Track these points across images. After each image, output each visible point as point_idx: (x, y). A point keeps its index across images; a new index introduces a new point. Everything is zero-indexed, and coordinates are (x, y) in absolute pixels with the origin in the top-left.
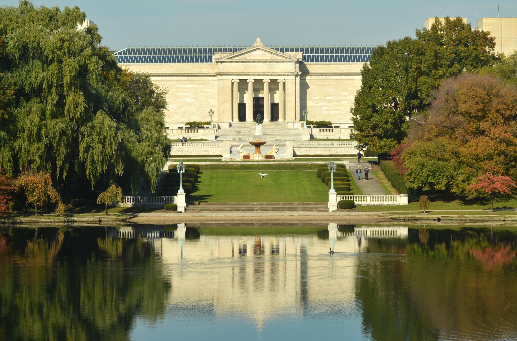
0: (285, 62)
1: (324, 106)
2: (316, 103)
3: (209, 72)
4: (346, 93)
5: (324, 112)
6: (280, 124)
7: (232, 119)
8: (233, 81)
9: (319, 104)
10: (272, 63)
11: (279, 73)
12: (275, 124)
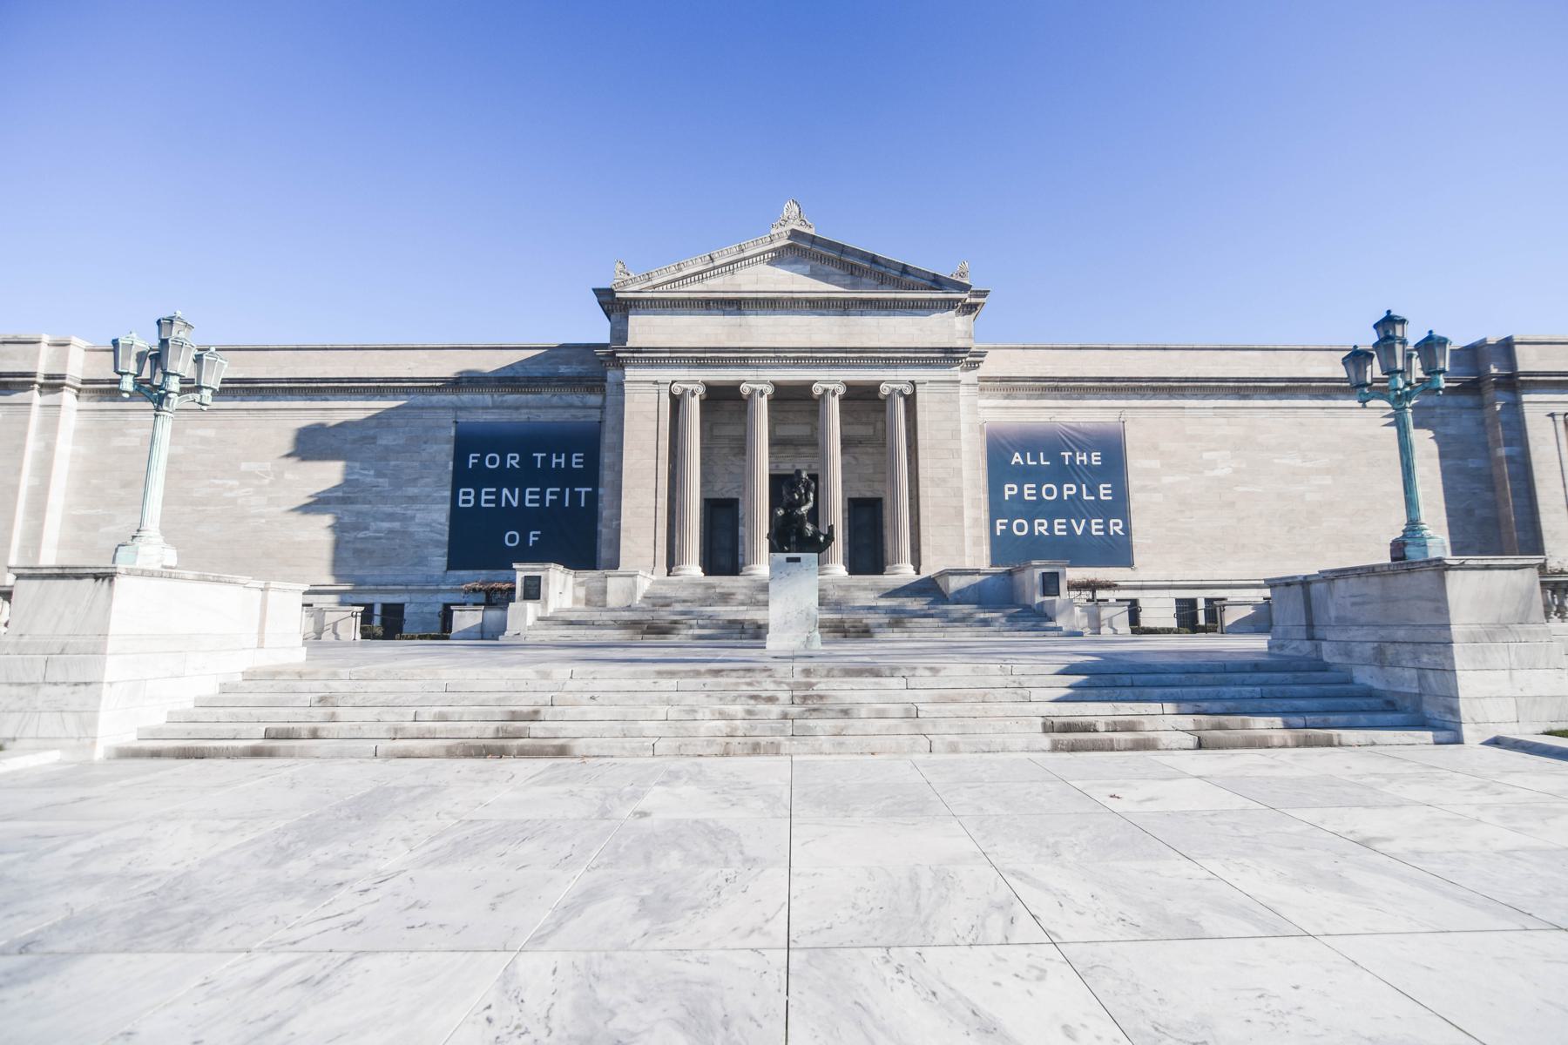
4: (1155, 464)
8: (677, 390)
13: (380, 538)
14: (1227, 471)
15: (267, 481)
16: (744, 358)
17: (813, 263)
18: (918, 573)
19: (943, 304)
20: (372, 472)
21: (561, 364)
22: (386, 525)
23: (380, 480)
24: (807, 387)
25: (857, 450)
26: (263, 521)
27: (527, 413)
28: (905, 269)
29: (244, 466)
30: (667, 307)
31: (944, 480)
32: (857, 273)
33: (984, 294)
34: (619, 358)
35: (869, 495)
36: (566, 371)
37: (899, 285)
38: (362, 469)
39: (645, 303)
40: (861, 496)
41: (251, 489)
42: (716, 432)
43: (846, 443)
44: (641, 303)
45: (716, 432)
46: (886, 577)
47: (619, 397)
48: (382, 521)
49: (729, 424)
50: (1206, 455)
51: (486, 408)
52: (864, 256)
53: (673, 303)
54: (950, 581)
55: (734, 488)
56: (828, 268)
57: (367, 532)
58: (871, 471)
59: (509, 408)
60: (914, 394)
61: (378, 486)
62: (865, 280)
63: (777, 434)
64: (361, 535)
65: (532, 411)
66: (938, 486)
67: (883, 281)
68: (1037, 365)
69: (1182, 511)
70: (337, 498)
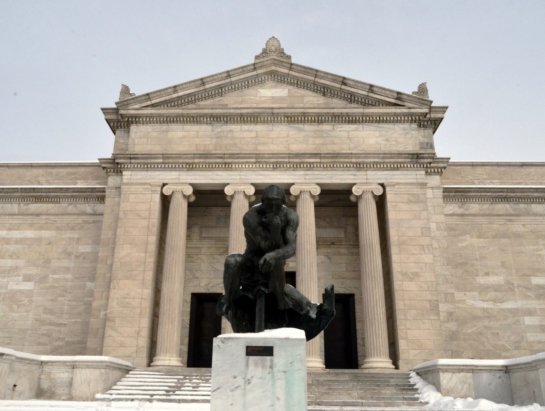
1: (530, 313)
2: (495, 301)
5: (531, 337)
8: (167, 191)
10: (326, 127)
11: (357, 156)
12: (357, 379)
16: (229, 163)
17: (290, 87)
18: (397, 368)
21: (80, 179)
24: (286, 189)
27: (46, 219)
31: (416, 274)
34: (118, 163)
43: (320, 243)
44: (141, 119)
46: (365, 371)
47: (117, 199)
49: (216, 227)
53: (168, 119)
54: (441, 378)
58: (344, 269)
59: (32, 215)
66: (411, 280)
68: (485, 179)
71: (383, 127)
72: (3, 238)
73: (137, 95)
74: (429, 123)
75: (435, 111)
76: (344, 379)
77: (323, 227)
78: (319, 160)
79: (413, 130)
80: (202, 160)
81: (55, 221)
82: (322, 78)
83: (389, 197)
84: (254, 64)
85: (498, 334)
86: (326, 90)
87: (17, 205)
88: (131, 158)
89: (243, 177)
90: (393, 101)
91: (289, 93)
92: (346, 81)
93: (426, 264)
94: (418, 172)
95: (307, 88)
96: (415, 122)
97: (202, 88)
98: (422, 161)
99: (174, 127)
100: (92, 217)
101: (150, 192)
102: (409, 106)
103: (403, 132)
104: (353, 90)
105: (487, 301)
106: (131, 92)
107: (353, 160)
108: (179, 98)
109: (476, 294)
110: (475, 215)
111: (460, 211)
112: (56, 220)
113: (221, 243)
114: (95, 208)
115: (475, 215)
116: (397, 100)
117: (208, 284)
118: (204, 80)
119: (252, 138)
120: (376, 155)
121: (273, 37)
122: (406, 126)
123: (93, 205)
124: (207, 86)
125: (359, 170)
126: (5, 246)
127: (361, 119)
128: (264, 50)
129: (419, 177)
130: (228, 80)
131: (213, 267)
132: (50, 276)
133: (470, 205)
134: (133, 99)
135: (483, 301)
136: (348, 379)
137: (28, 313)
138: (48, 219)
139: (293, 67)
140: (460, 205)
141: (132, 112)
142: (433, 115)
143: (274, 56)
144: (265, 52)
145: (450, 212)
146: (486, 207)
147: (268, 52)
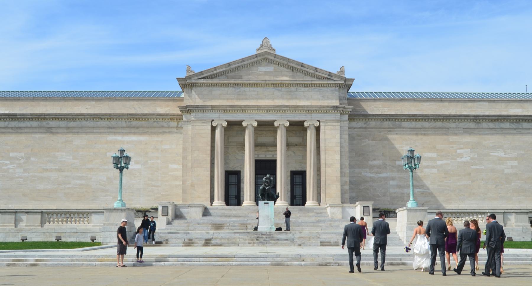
0: (321, 86)
3: (171, 112)
4: (434, 155)
6: (309, 210)
7: (212, 200)
8: (214, 124)
9: (382, 175)
10: (293, 89)
11: (307, 106)
12: (301, 210)
13: (76, 188)
14: (468, 159)
15: (22, 161)
16: (244, 110)
17: (275, 66)
19: (333, 85)
20: (71, 157)
22: (78, 182)
23: (75, 161)
25: (294, 149)
26: (22, 180)
28: (316, 69)
29: (12, 154)
30: (210, 86)
32: (295, 71)
33: (353, 80)
35: (300, 169)
36: (160, 110)
37: (313, 76)
38: (66, 156)
39: (200, 85)
40: (296, 170)
41: (15, 165)
42: (230, 140)
44: (198, 85)
45: (230, 140)
48: (77, 180)
50: (458, 151)
51: (123, 127)
52: (298, 63)
55: (239, 166)
56: (282, 68)
57: (70, 185)
59: (134, 127)
60: (319, 127)
61: (74, 164)
62: (298, 74)
63: (258, 141)
64: (67, 186)
65: (145, 129)
67: (306, 73)
69: (446, 177)
70: (56, 169)
71: (321, 89)
72: (120, 141)
73: (196, 72)
74: (345, 86)
75: (348, 81)
76: (296, 210)
77: (291, 136)
78: (288, 109)
79: (336, 91)
80: (231, 108)
81: (147, 131)
82: (291, 63)
83: (322, 127)
84: (256, 55)
85: (376, 189)
86: (293, 69)
87: (125, 122)
88: (195, 107)
89: (252, 116)
90: (327, 76)
91: (274, 69)
92: (303, 65)
93: (336, 160)
94: (336, 115)
95: (284, 67)
96: (338, 87)
97: (229, 68)
98: (338, 109)
99: (215, 88)
100: (168, 129)
101: (206, 125)
102: (335, 80)
103: (332, 92)
104: (307, 70)
105: (373, 173)
106: (192, 70)
107: (305, 109)
108: (216, 74)
109: (368, 169)
110: (372, 128)
111: (364, 126)
112: (148, 130)
113: (239, 145)
114: (169, 124)
115: (372, 128)
116: (329, 76)
117: (233, 166)
118: (230, 64)
119: (255, 95)
120: (316, 107)
121: (266, 37)
122: (333, 88)
123: (167, 122)
124: (232, 67)
125: (308, 113)
126: (122, 145)
127: (310, 85)
128: (261, 45)
129: (337, 117)
130: (243, 63)
131: (235, 157)
132: (149, 161)
133: (370, 122)
134: (193, 74)
135: (371, 173)
136: (297, 210)
137: (140, 181)
138: (143, 130)
139: (276, 56)
140: (365, 122)
141: (194, 81)
142: (347, 83)
143: (265, 50)
144: (262, 46)
145: (359, 126)
146: (378, 123)
147: (263, 47)
